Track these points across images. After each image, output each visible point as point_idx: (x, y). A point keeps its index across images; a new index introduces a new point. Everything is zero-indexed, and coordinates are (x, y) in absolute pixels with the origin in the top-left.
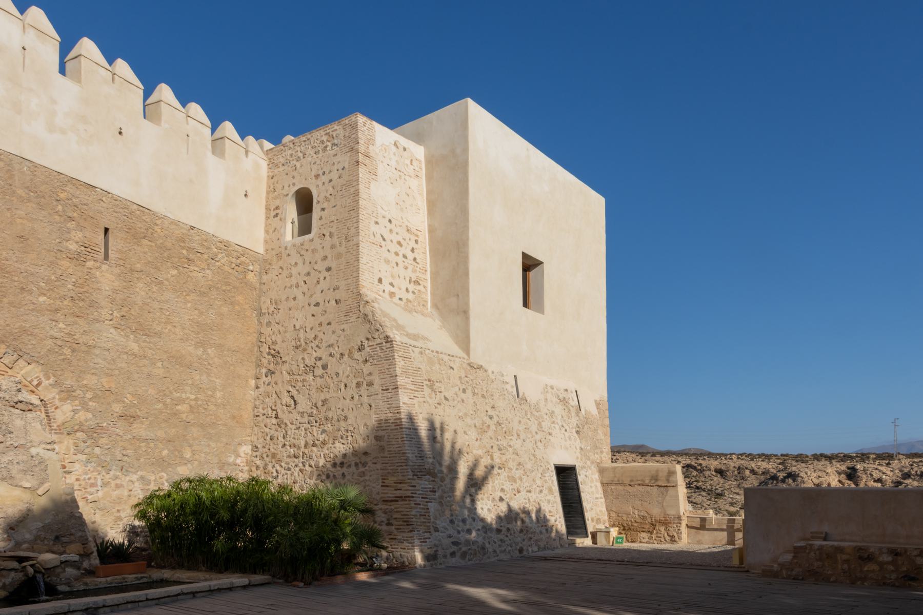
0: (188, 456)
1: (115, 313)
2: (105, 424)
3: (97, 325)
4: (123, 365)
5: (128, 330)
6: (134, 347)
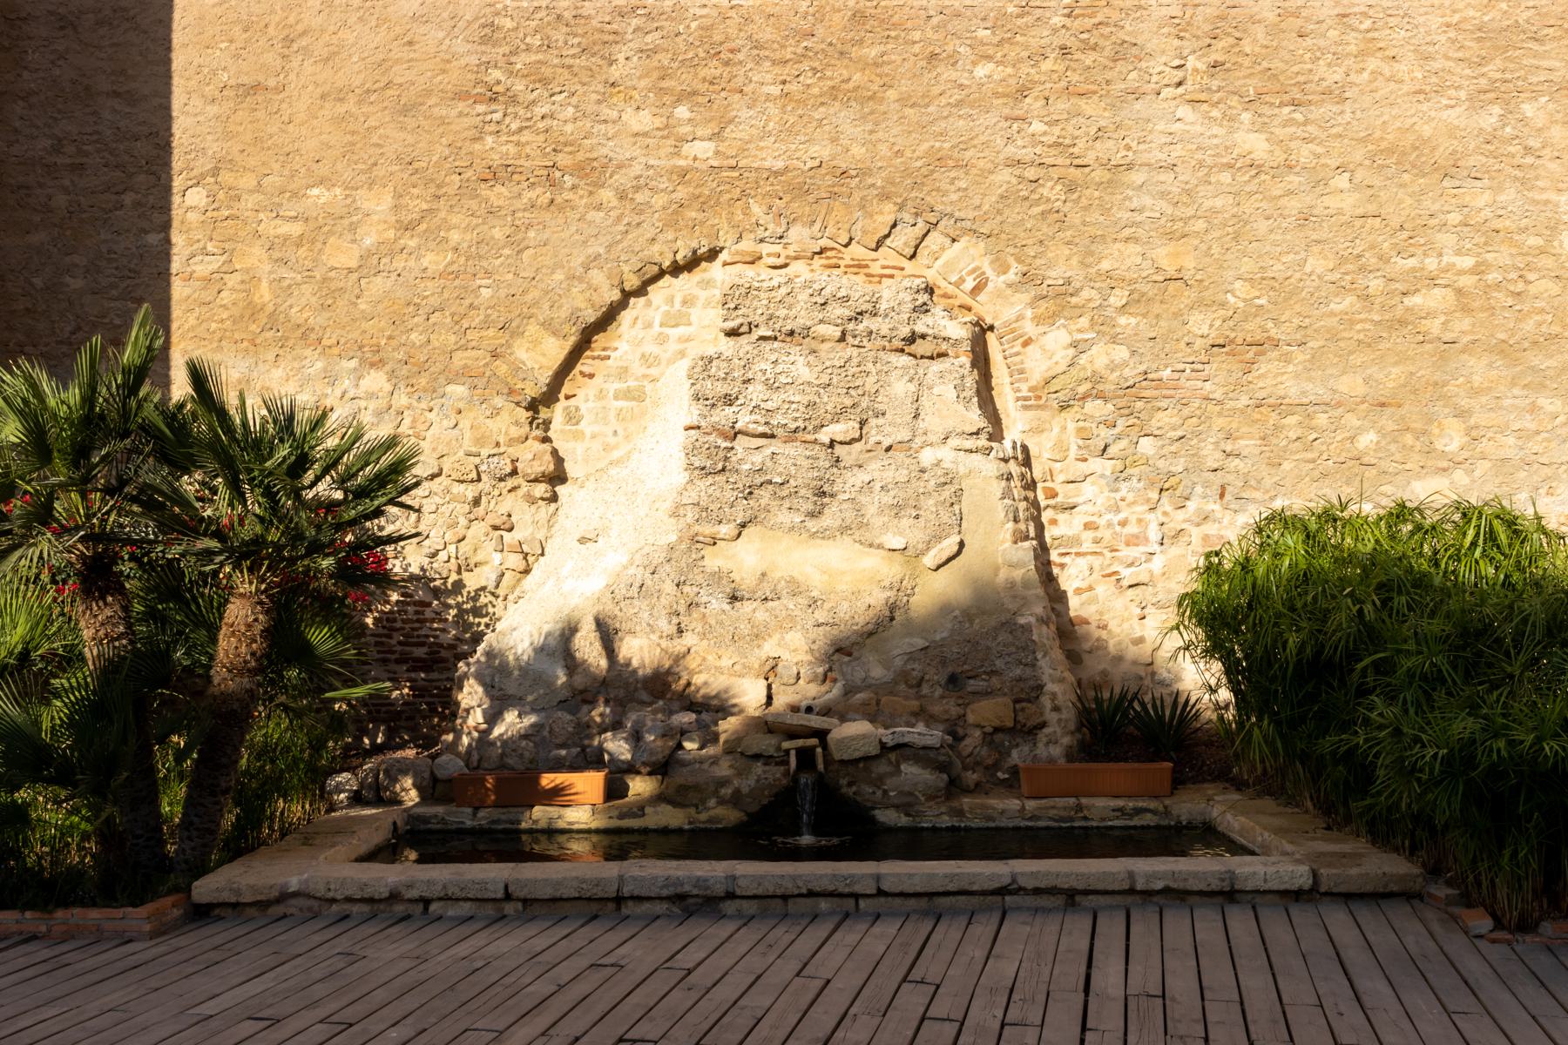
0: (1453, 447)
1: (1192, 62)
3: (1138, 106)
4: (1219, 203)
5: (1234, 101)
6: (1255, 144)
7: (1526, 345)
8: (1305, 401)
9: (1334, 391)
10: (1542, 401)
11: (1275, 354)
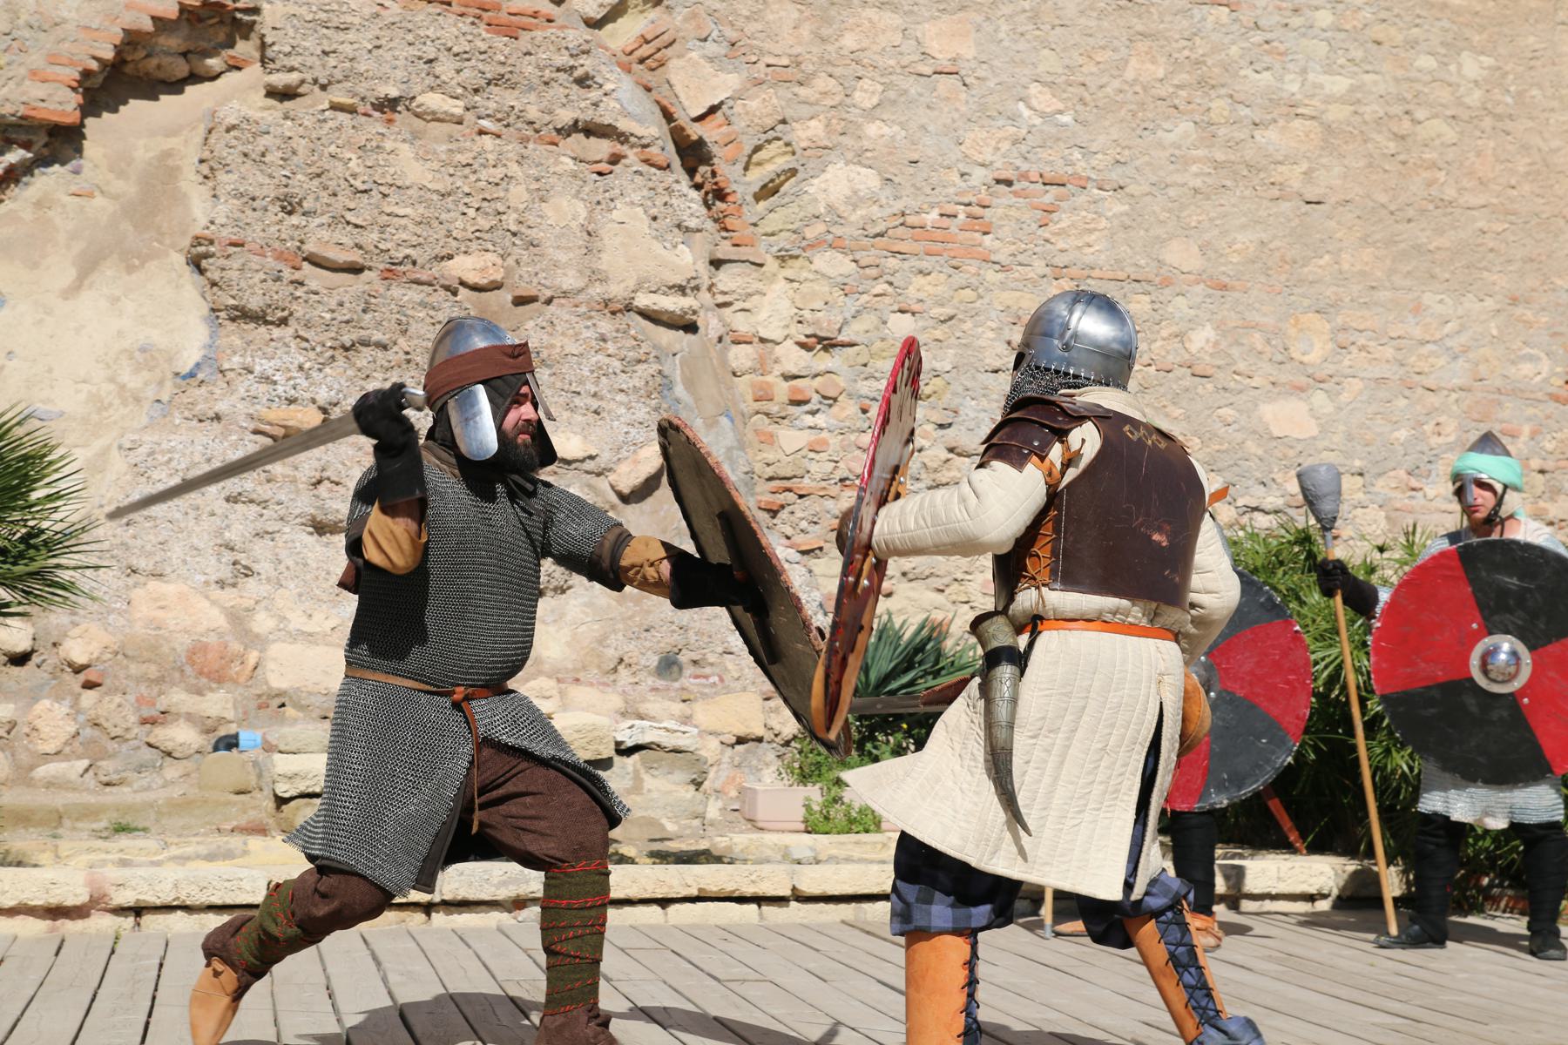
2: (932, 217)
7: (1411, 213)
8: (1121, 275)
10: (1429, 299)
11: (1082, 199)
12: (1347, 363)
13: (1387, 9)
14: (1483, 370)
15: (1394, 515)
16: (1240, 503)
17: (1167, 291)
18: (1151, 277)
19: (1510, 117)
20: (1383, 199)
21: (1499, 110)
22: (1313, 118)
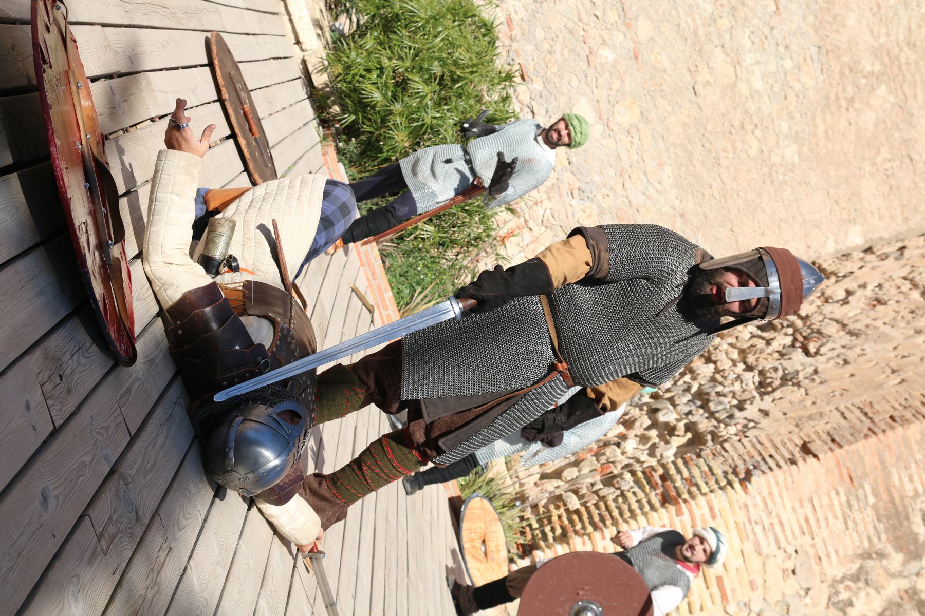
7: (707, 145)
9: (637, 19)
10: (668, 169)
12: (621, 136)
13: (804, 96)
14: (643, 210)
15: (556, 187)
16: (533, 103)
17: (624, 28)
18: (628, 16)
19: (772, 181)
20: (709, 128)
21: (774, 174)
22: (736, 76)
